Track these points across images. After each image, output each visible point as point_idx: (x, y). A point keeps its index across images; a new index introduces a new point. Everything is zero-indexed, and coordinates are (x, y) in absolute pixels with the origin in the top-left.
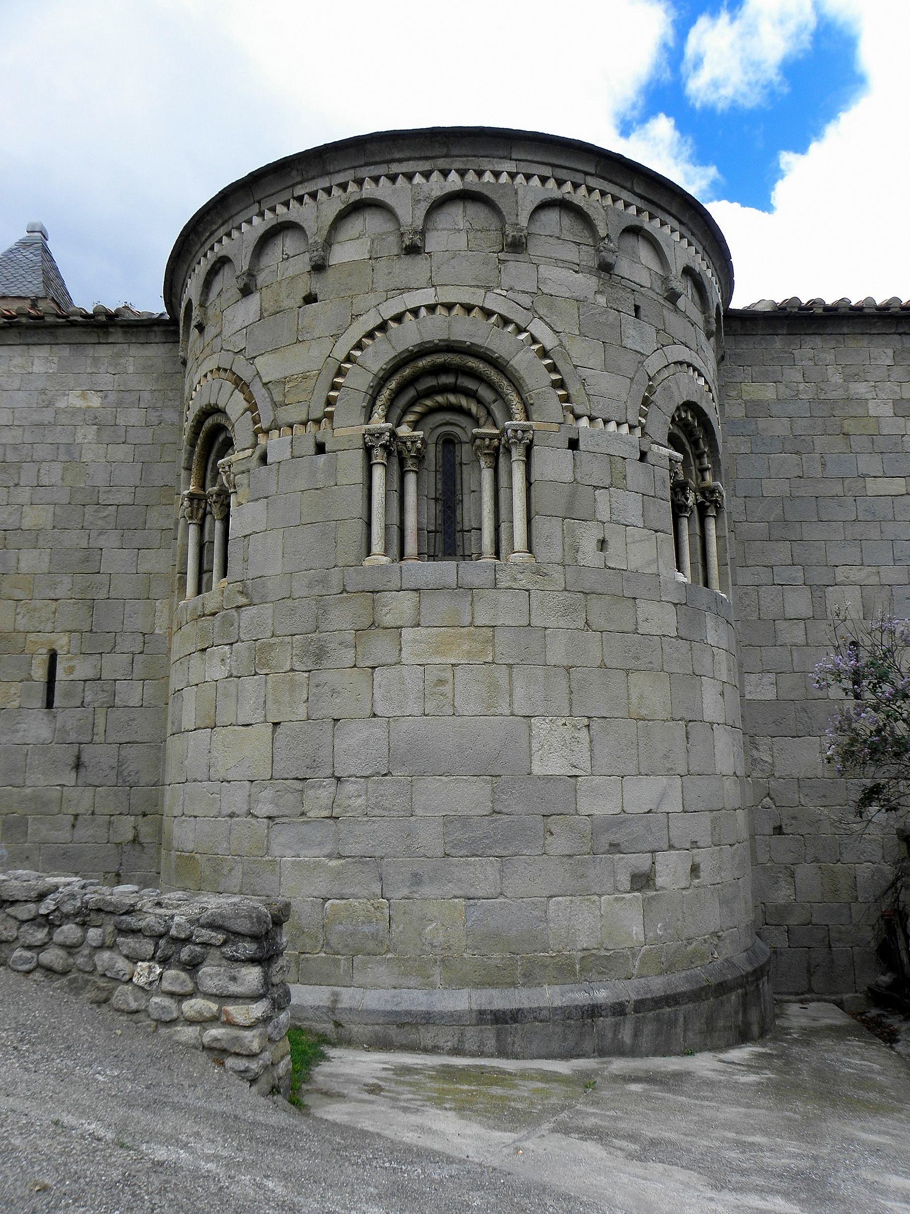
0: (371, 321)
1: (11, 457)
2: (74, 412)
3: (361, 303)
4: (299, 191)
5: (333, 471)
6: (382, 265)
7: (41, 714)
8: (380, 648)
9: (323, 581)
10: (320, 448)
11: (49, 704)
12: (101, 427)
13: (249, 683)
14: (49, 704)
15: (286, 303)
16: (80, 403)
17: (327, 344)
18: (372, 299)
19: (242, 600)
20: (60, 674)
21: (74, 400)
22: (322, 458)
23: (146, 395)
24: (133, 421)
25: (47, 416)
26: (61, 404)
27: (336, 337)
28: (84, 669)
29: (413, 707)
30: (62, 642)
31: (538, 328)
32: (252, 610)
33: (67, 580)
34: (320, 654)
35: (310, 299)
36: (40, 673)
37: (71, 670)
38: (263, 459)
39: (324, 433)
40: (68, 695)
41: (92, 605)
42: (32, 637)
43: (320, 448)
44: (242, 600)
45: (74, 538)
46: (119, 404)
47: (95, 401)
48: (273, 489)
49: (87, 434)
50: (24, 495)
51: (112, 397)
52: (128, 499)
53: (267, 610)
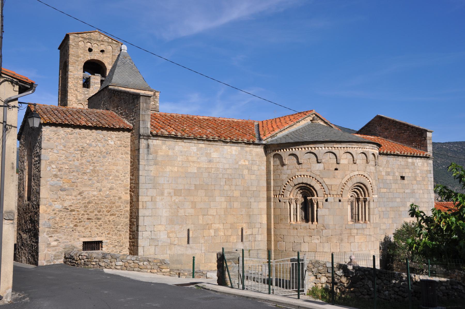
0: (348, 177)
1: (230, 177)
2: (243, 166)
3: (347, 172)
4: (335, 146)
5: (343, 206)
6: (350, 165)
7: (241, 243)
8: (352, 239)
9: (342, 227)
10: (340, 201)
11: (242, 241)
12: (249, 170)
13: (326, 244)
14: (242, 241)
15: (331, 169)
16: (244, 163)
17: (340, 180)
18: (349, 172)
19: (323, 228)
20: (244, 233)
21: (242, 162)
22: (340, 203)
23: (258, 162)
24: (255, 169)
25: (237, 167)
26: (240, 163)
27: (342, 179)
28: (249, 232)
29: (357, 250)
30: (245, 226)
31: (370, 179)
32: (326, 230)
33: (244, 210)
34: (342, 240)
35: (336, 169)
36: (240, 234)
37: (246, 232)
38: (327, 200)
39: (341, 198)
40: (246, 238)
41: (250, 216)
42: (238, 224)
43: (340, 201)
44: (323, 228)
45: (245, 199)
46: (252, 164)
47: (247, 163)
48: (330, 207)
49: (246, 172)
50: (233, 188)
51: (251, 162)
52: (255, 189)
53: (330, 231)
